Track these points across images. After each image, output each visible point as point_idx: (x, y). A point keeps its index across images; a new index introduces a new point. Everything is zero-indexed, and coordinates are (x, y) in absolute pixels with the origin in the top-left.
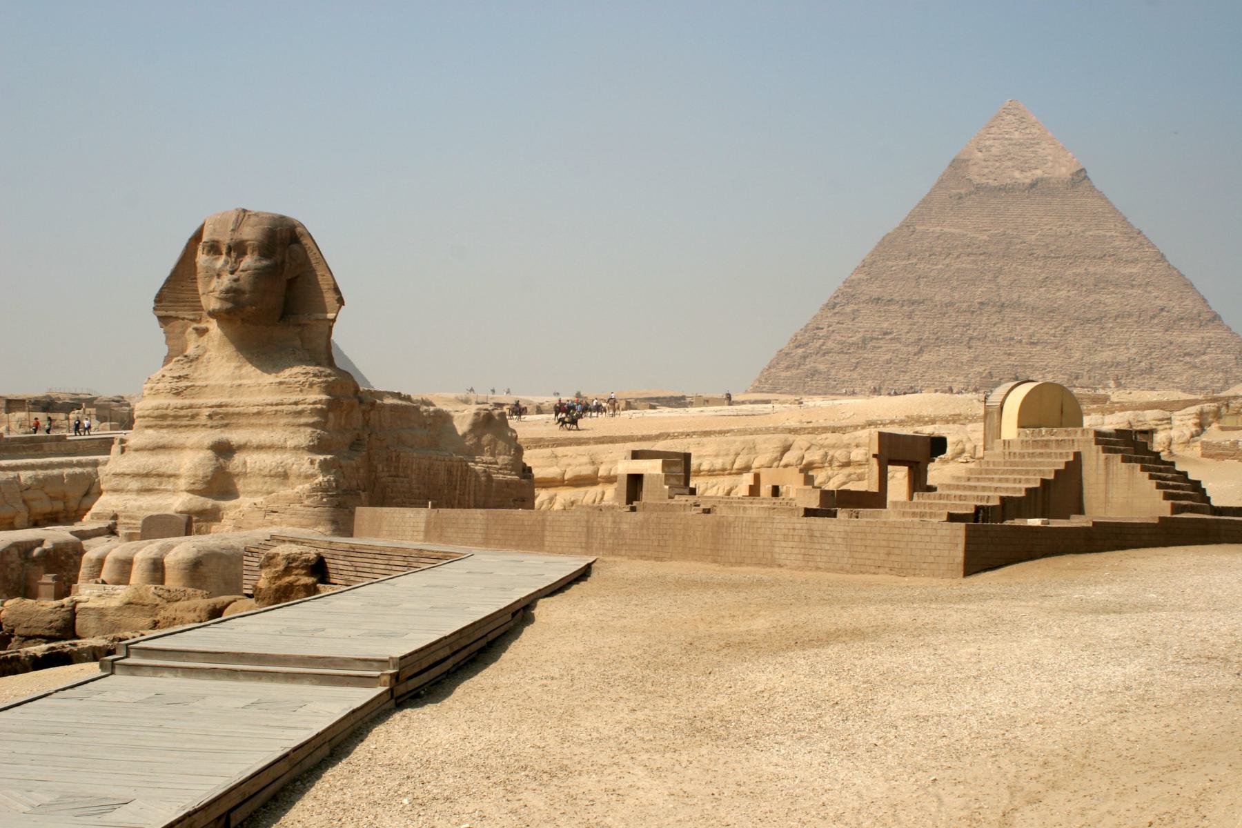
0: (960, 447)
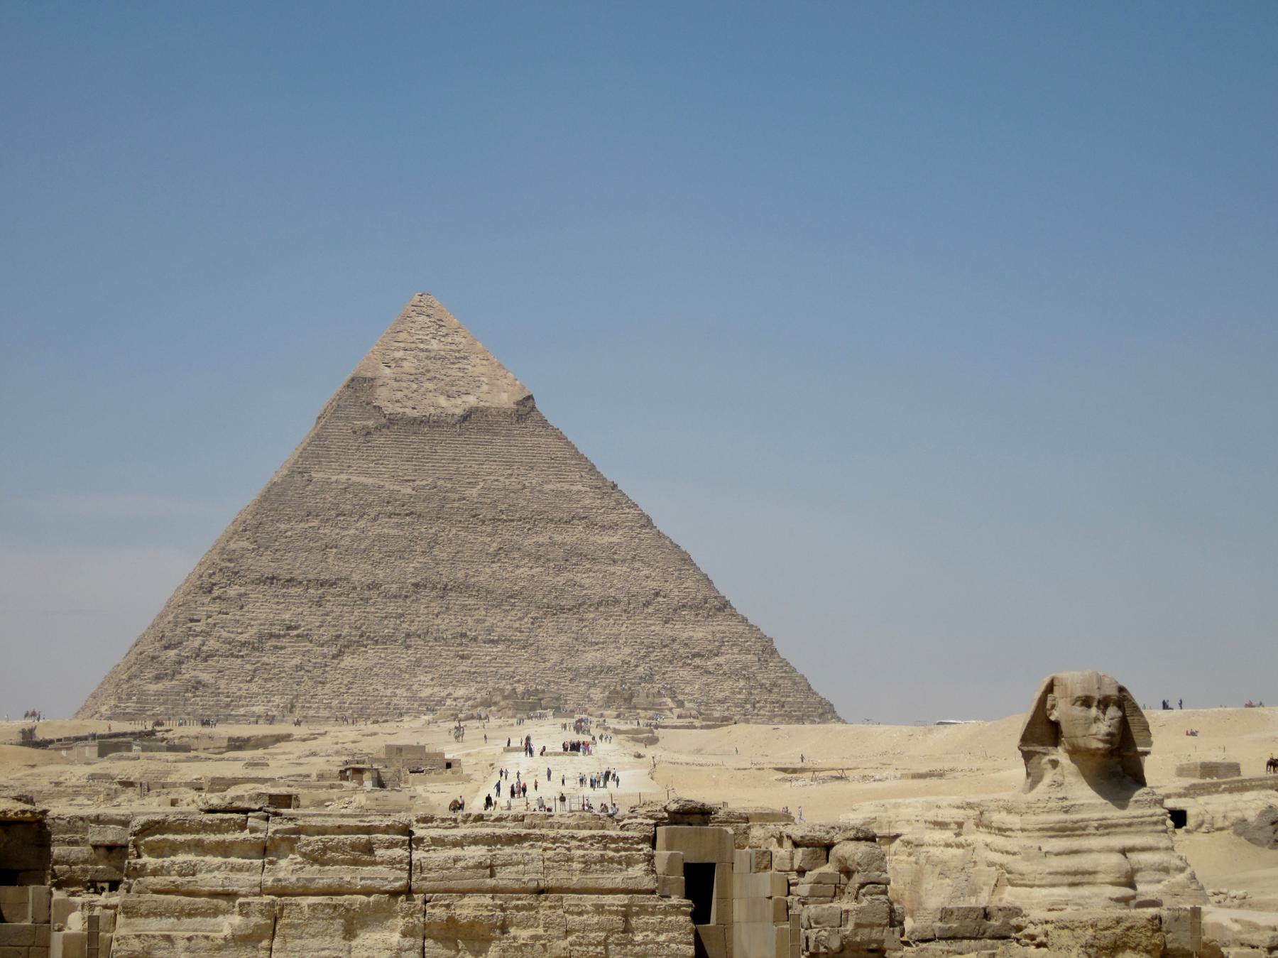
0: (1200, 818)
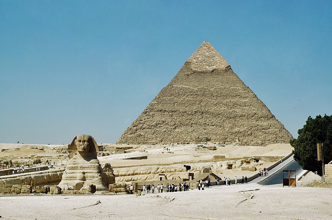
0: (193, 168)
